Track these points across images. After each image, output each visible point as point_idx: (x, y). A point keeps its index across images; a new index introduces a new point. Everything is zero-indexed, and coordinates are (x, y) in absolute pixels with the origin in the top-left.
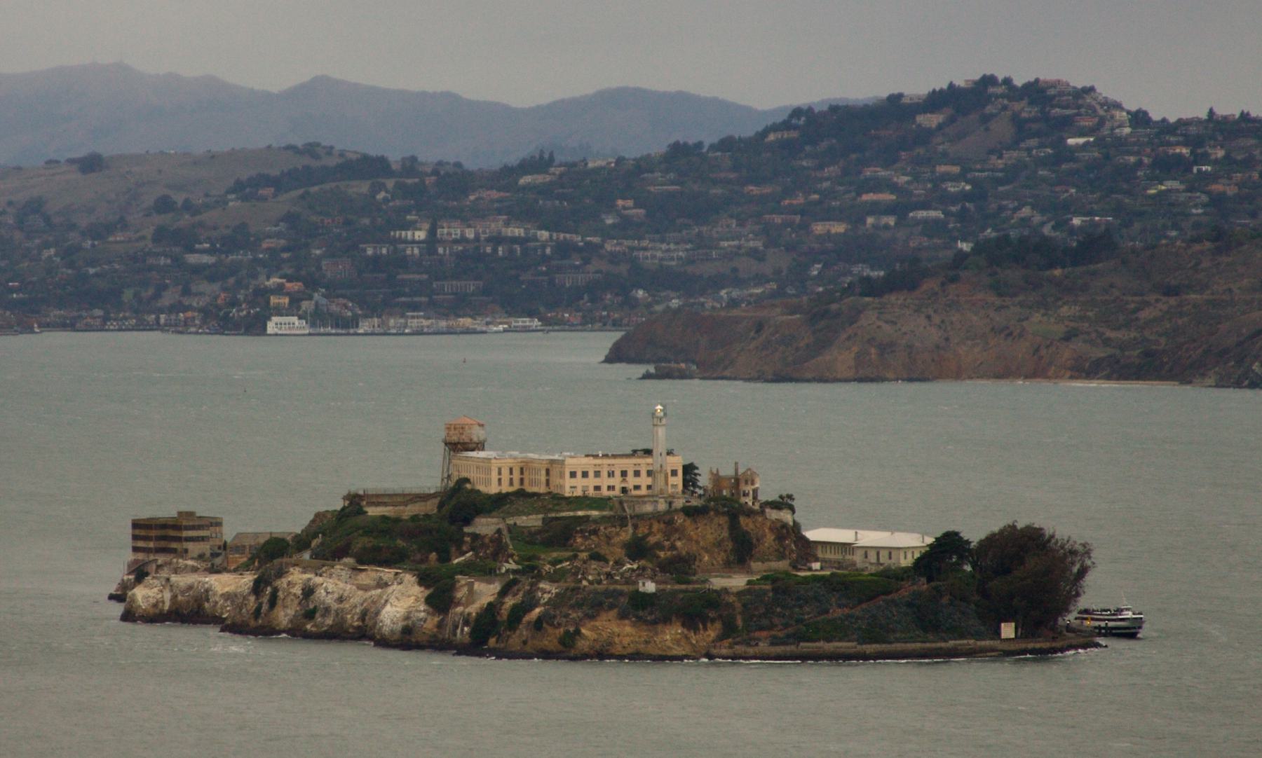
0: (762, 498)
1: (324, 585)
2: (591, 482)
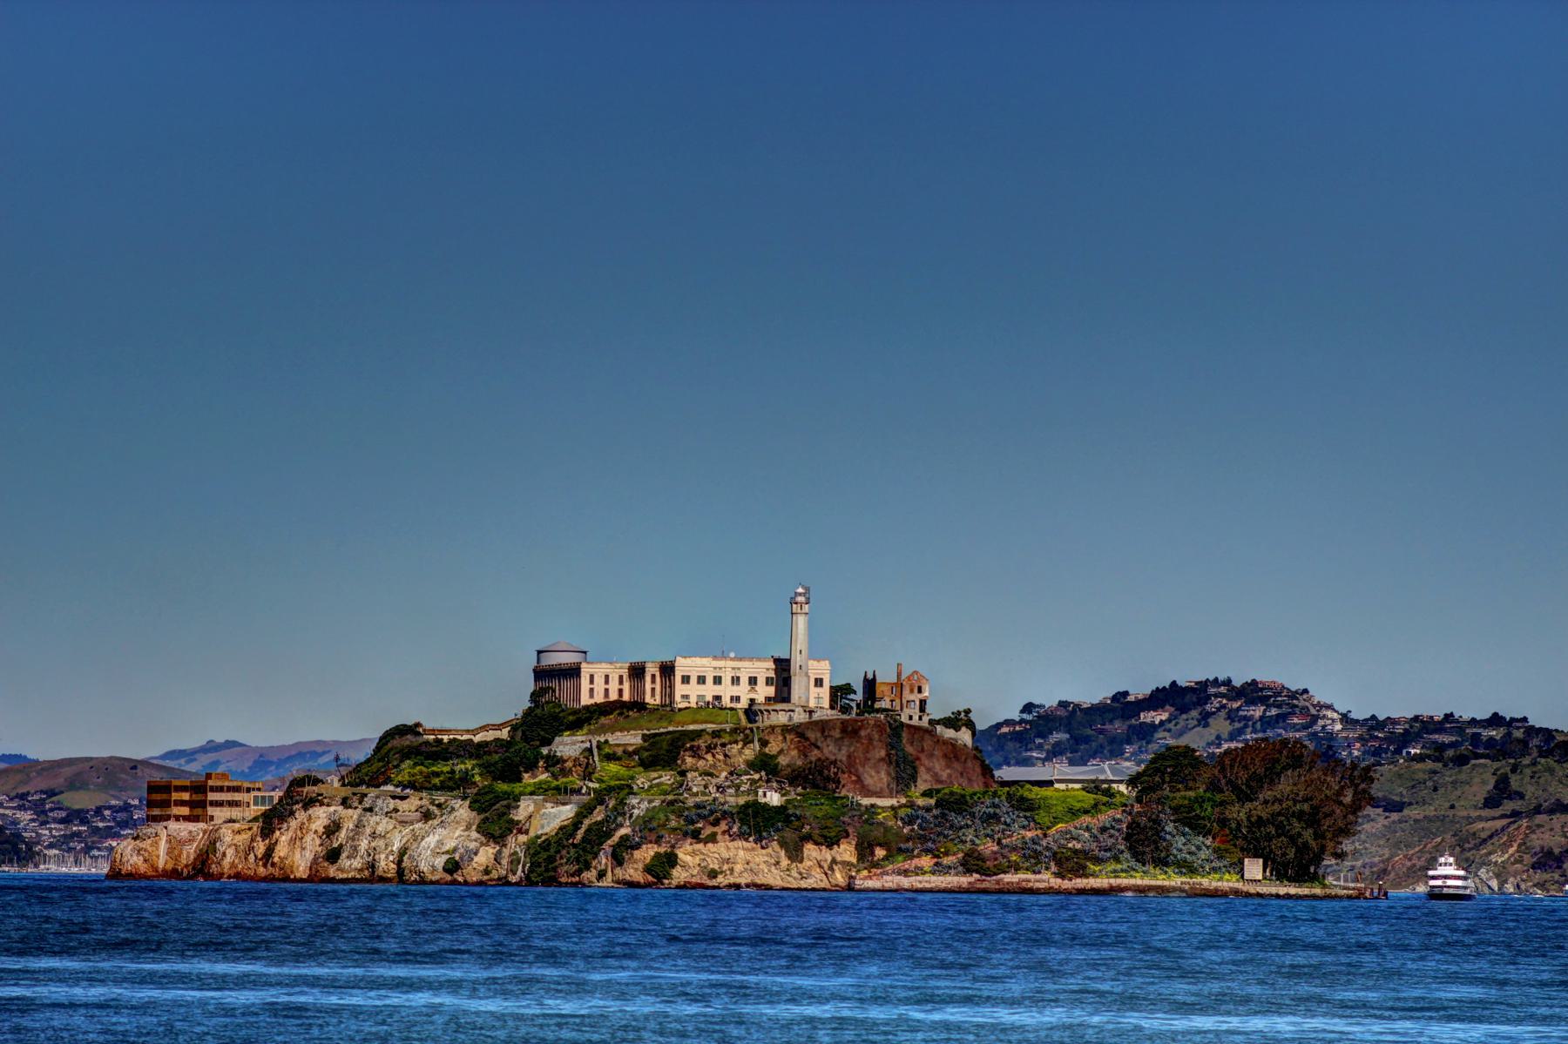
0: (936, 711)
2: (709, 691)
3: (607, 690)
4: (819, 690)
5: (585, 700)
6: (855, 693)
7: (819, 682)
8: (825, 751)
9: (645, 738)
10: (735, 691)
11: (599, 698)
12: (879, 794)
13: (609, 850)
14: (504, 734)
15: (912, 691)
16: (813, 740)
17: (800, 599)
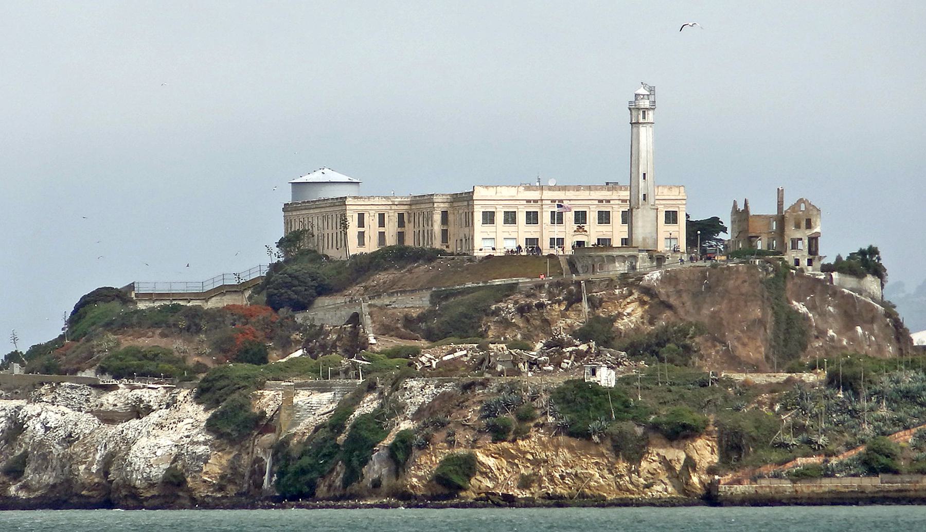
0: (829, 253)
1: (42, 417)
2: (522, 232)
3: (382, 234)
4: (672, 228)
5: (354, 249)
6: (724, 230)
7: (671, 217)
8: (681, 312)
9: (437, 297)
10: (557, 231)
11: (372, 246)
12: (756, 368)
13: (384, 453)
14: (242, 300)
15: (798, 226)
16: (663, 298)
17: (645, 103)
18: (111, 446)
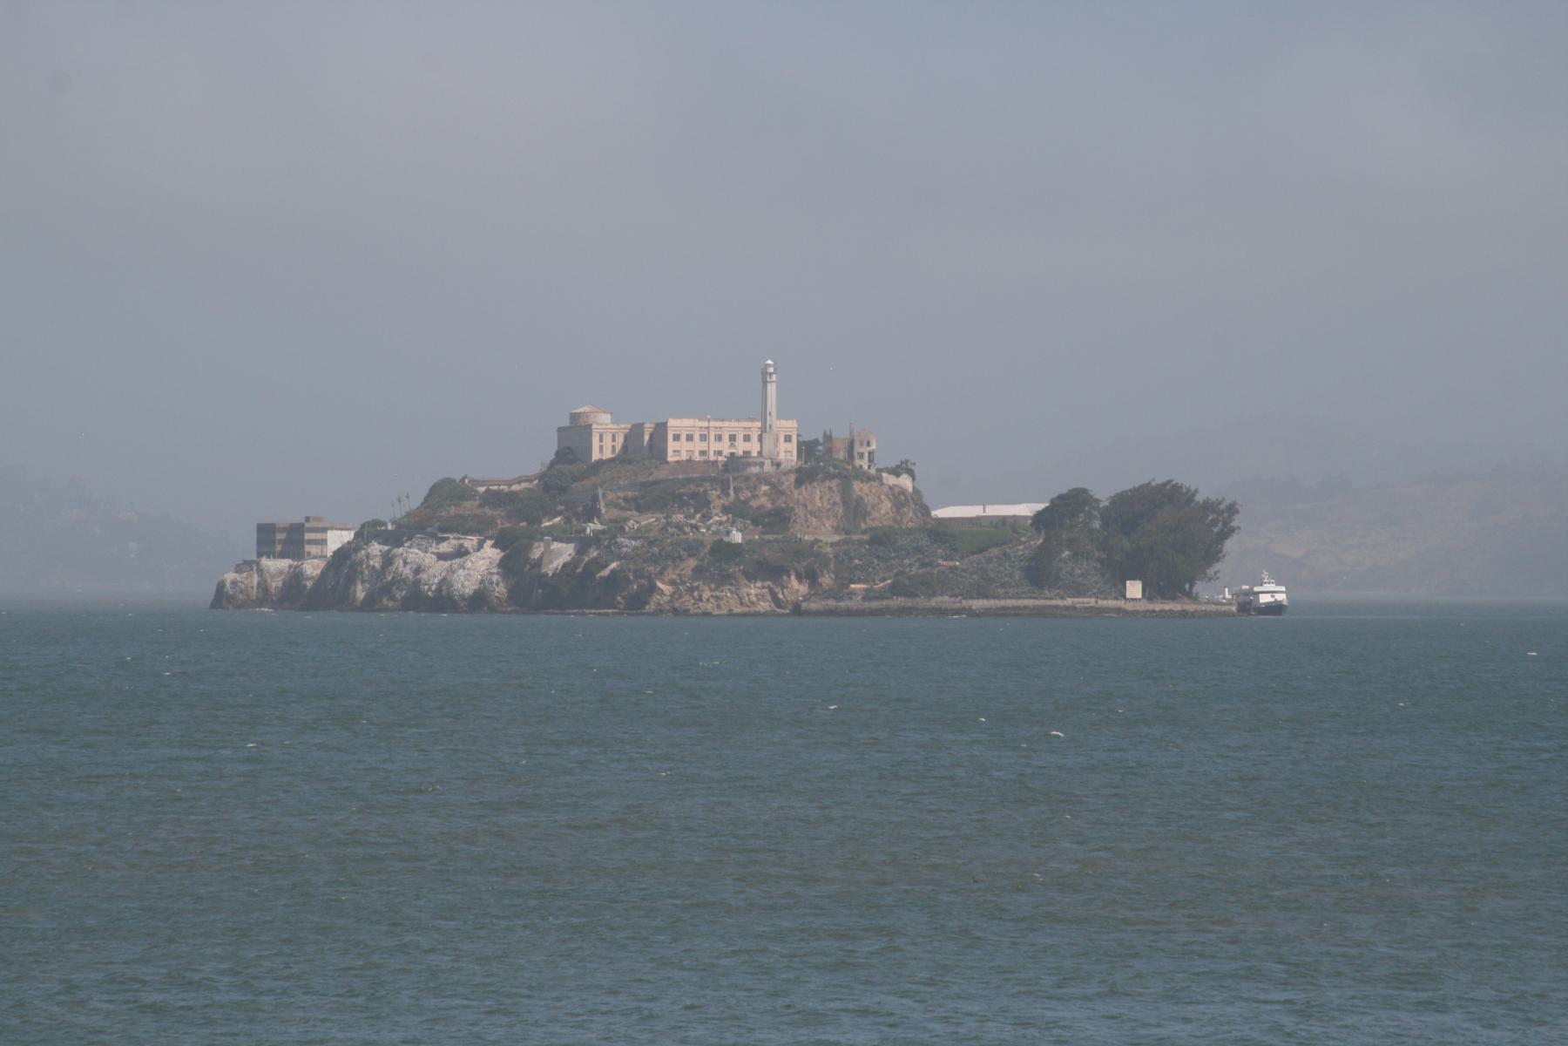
2: (698, 446)
4: (788, 445)
11: (608, 455)
15: (861, 444)
17: (771, 370)
18: (443, 574)
